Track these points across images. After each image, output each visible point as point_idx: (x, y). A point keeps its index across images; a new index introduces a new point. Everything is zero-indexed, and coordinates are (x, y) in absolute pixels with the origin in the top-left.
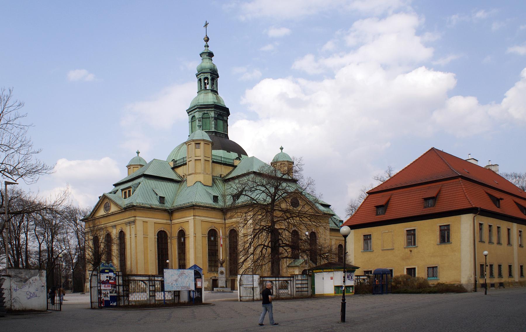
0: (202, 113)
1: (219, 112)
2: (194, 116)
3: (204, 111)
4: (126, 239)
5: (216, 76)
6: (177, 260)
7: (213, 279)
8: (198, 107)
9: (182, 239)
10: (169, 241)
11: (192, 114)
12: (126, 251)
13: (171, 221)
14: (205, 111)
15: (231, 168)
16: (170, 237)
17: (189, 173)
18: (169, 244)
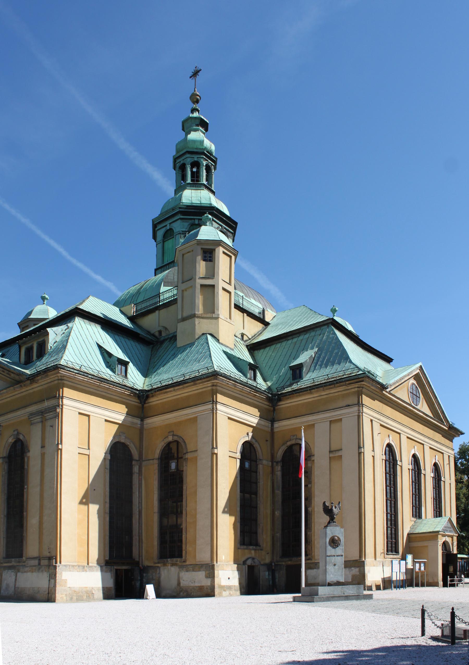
0: (189, 223)
1: (221, 226)
2: (171, 229)
3: (193, 221)
4: (28, 460)
5: (214, 164)
6: (156, 518)
7: (250, 564)
8: (181, 210)
9: (173, 466)
10: (136, 469)
11: (166, 226)
12: (25, 490)
13: (142, 420)
14: (194, 219)
15: (260, 326)
16: (137, 459)
17: (185, 315)
18: (135, 478)
